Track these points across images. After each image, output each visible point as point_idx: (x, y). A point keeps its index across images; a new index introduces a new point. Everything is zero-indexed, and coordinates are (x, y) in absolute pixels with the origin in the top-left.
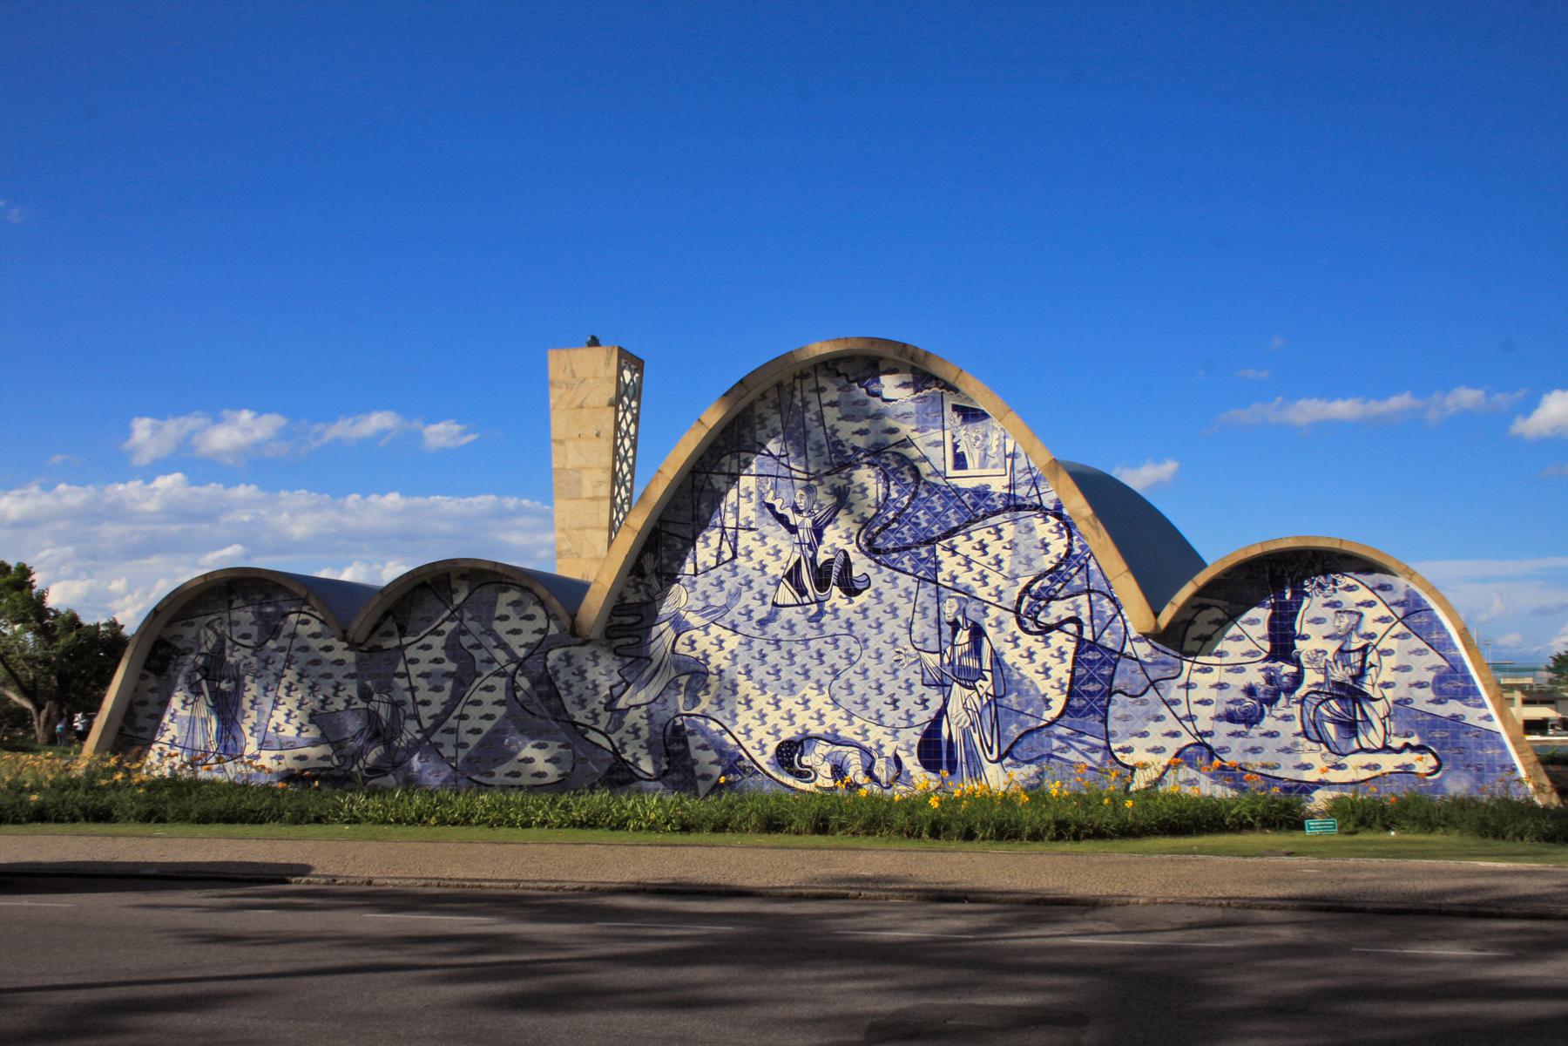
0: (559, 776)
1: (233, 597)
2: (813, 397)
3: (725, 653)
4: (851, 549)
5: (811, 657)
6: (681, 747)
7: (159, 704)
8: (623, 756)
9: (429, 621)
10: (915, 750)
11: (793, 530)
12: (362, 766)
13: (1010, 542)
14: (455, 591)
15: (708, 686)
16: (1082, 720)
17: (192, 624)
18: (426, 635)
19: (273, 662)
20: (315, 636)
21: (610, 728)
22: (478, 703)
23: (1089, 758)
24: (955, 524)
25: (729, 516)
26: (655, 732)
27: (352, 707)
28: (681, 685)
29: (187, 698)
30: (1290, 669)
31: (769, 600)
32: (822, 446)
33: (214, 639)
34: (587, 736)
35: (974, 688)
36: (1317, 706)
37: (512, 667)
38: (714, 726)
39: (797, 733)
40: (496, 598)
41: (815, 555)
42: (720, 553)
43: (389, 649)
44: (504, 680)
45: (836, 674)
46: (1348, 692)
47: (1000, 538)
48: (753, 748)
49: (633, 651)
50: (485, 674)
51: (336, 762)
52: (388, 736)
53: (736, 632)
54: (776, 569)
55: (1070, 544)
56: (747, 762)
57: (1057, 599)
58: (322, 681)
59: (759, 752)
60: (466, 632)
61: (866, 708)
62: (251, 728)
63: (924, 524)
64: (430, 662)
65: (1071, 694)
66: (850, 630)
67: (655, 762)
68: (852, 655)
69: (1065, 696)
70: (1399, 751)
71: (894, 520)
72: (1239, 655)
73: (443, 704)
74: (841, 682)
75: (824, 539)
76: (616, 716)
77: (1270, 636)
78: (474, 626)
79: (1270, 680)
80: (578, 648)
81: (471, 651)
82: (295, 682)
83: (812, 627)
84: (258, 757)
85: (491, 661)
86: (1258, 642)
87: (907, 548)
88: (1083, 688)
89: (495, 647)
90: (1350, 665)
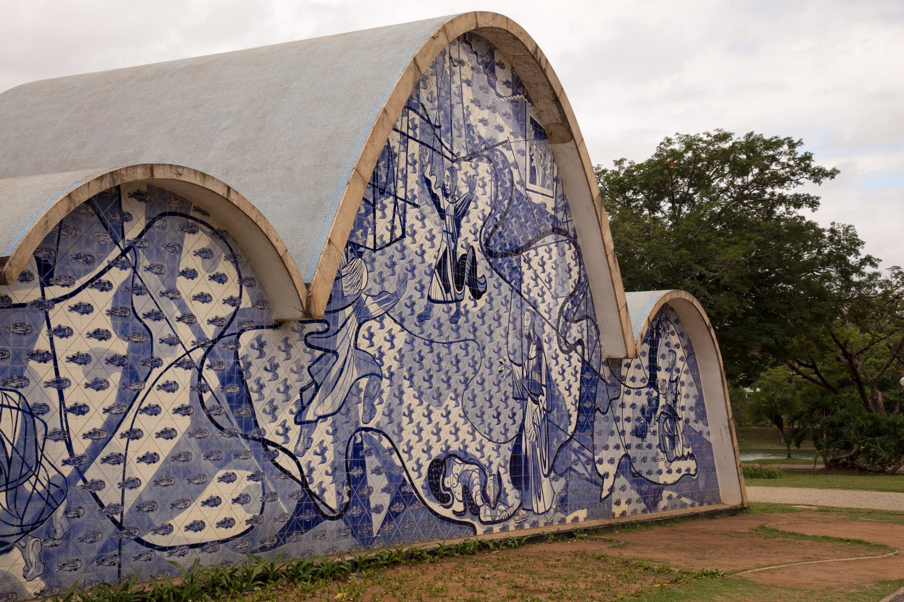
0: (248, 522)
3: (394, 352)
4: (476, 245)
5: (452, 362)
6: (360, 472)
8: (311, 487)
9: (89, 261)
10: (508, 466)
11: (442, 214)
13: (555, 262)
14: (127, 217)
15: (382, 392)
16: (583, 434)
18: (84, 286)
21: (300, 448)
23: (586, 470)
24: (530, 238)
25: (400, 183)
26: (340, 453)
28: (360, 390)
30: (655, 394)
31: (426, 293)
34: (277, 460)
35: (536, 402)
37: (198, 354)
38: (386, 444)
39: (442, 449)
40: (183, 241)
41: (456, 247)
43: (23, 305)
44: (189, 372)
45: (466, 382)
47: (550, 258)
48: (413, 469)
49: (321, 342)
53: (402, 327)
54: (431, 258)
55: (579, 273)
56: (408, 489)
57: (576, 322)
59: (416, 474)
60: (140, 290)
61: (483, 421)
64: (90, 335)
65: (580, 410)
66: (475, 336)
67: (338, 493)
68: (476, 363)
69: (577, 412)
73: (106, 411)
74: (468, 394)
75: (462, 231)
76: (305, 430)
77: (650, 366)
78: (151, 280)
79: (649, 401)
80: (271, 330)
81: (148, 322)
83: (452, 329)
85: (173, 341)
89: (179, 319)
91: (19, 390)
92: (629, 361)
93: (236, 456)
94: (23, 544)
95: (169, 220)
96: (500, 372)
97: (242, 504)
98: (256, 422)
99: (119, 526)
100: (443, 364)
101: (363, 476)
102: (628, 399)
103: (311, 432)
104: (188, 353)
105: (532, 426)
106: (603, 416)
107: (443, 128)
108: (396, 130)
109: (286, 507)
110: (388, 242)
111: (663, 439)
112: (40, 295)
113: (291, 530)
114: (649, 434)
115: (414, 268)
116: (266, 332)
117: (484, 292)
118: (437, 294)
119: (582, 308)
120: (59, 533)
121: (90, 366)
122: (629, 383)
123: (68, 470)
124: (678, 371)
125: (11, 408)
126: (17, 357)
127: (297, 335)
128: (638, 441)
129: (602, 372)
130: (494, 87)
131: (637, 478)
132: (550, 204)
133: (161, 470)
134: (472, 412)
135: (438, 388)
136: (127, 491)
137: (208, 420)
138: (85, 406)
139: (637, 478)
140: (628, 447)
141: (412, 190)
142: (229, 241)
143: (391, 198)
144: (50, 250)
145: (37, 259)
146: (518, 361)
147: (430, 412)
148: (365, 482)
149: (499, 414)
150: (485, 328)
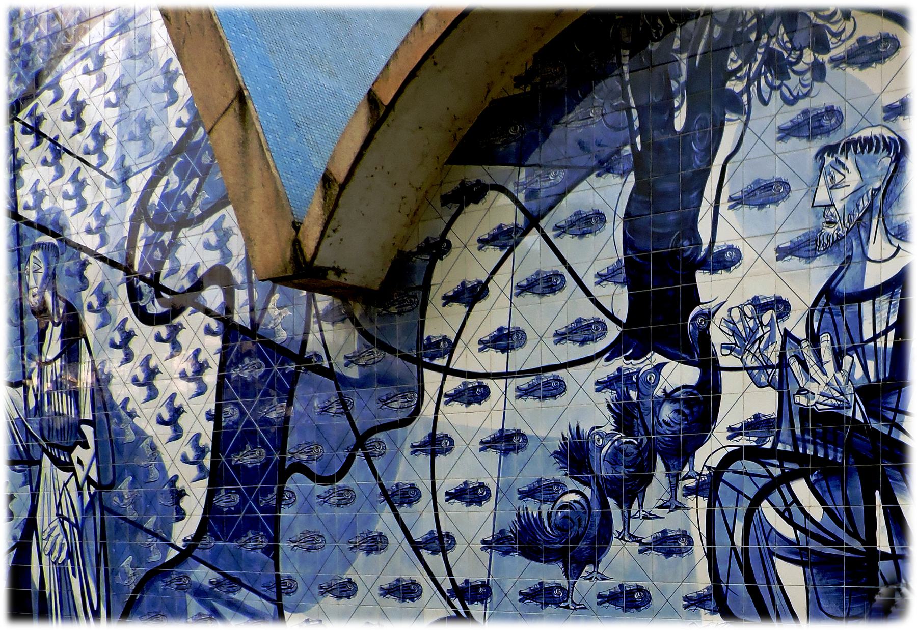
35: (67, 467)
36: (756, 502)
46: (851, 450)
69: (206, 482)
72: (549, 340)
86: (596, 291)
88: (236, 459)
90: (858, 347)
105: (56, 523)
106: (320, 489)
122: (465, 359)
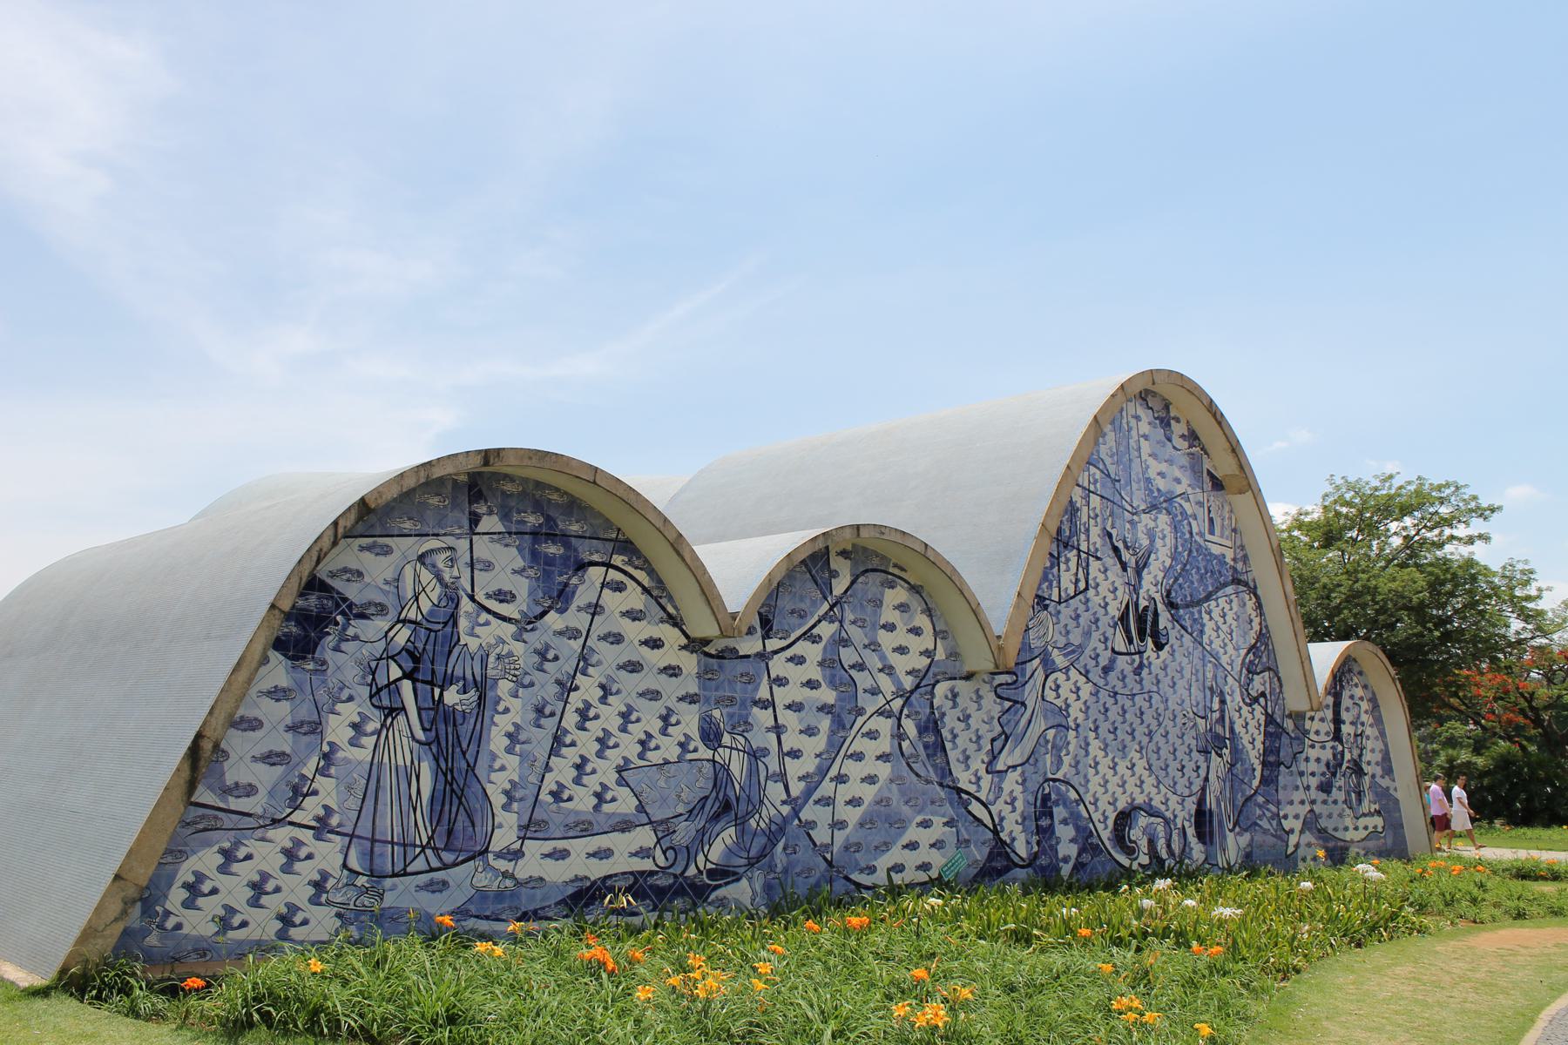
1: (481, 509)
2: (1133, 422)
3: (1080, 704)
4: (1158, 597)
6: (1048, 822)
7: (289, 728)
8: (1001, 834)
9: (802, 615)
10: (1193, 820)
11: (1124, 567)
12: (702, 869)
13: (1236, 613)
14: (834, 574)
15: (1068, 743)
17: (387, 551)
18: (798, 639)
19: (556, 658)
20: (634, 616)
21: (991, 797)
22: (858, 757)
23: (1271, 825)
24: (1210, 589)
25: (1083, 537)
27: (689, 756)
28: (1047, 742)
29: (364, 718)
31: (1109, 644)
32: (1139, 481)
33: (435, 593)
34: (970, 808)
35: (1220, 756)
37: (897, 704)
38: (1073, 795)
40: (883, 596)
41: (1138, 599)
42: (1077, 581)
43: (747, 657)
44: (889, 721)
45: (1150, 734)
48: (1099, 821)
50: (868, 714)
51: (661, 861)
52: (743, 808)
53: (1087, 678)
54: (1114, 611)
55: (1260, 624)
56: (1095, 840)
57: (1258, 674)
58: (642, 704)
59: (1102, 826)
60: (845, 642)
61: (1167, 773)
62: (506, 793)
63: (1196, 584)
64: (803, 685)
65: (1264, 764)
67: (1028, 843)
70: (1373, 815)
71: (1180, 574)
73: (817, 756)
75: (1143, 582)
78: (855, 633)
79: (1334, 756)
80: (963, 682)
81: (853, 672)
82: (595, 702)
84: (517, 855)
85: (875, 691)
87: (1187, 606)
89: (881, 670)
91: (745, 734)
92: (1313, 713)
93: (933, 802)
94: (750, 874)
95: (871, 575)
96: (1184, 724)
97: (938, 849)
98: (950, 770)
99: (830, 863)
100: (1127, 716)
101: (1051, 828)
102: (1313, 754)
103: (1002, 781)
104: (888, 702)
107: (1122, 482)
108: (1078, 485)
109: (979, 854)
110: (1072, 594)
111: (1349, 795)
112: (762, 647)
113: (984, 876)
114: (1334, 789)
115: (1097, 620)
116: (958, 683)
117: (1167, 644)
118: (1121, 646)
119: (1265, 659)
120: (779, 868)
121: (803, 713)
123: (786, 810)
124: (1363, 724)
125: (739, 750)
126: (743, 704)
127: (988, 686)
128: (1324, 796)
129: (1285, 725)
130: (1169, 440)
131: (1322, 834)
132: (1229, 555)
133: (864, 813)
134: (1156, 764)
135: (1123, 740)
136: (835, 831)
137: (907, 768)
138: (799, 750)
139: (1322, 834)
140: (1313, 802)
141: (1095, 543)
142: (924, 595)
143: (1075, 552)
144: (769, 606)
145: (760, 614)
146: (1202, 713)
147: (1116, 764)
148: (1053, 832)
149: (1183, 767)
150: (1168, 680)
